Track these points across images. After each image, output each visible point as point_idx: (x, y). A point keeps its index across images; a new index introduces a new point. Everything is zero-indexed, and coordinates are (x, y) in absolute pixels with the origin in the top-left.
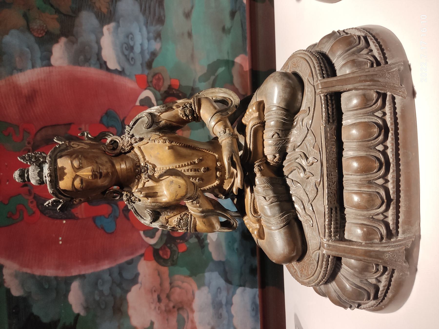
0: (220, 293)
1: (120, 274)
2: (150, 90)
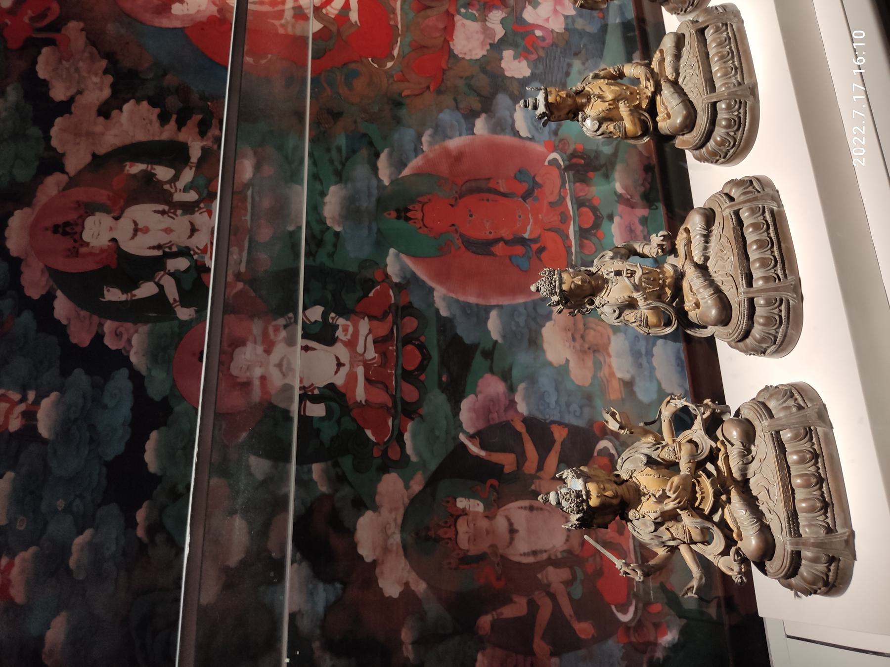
0: (639, 341)
1: (535, 309)
2: (557, 153)
